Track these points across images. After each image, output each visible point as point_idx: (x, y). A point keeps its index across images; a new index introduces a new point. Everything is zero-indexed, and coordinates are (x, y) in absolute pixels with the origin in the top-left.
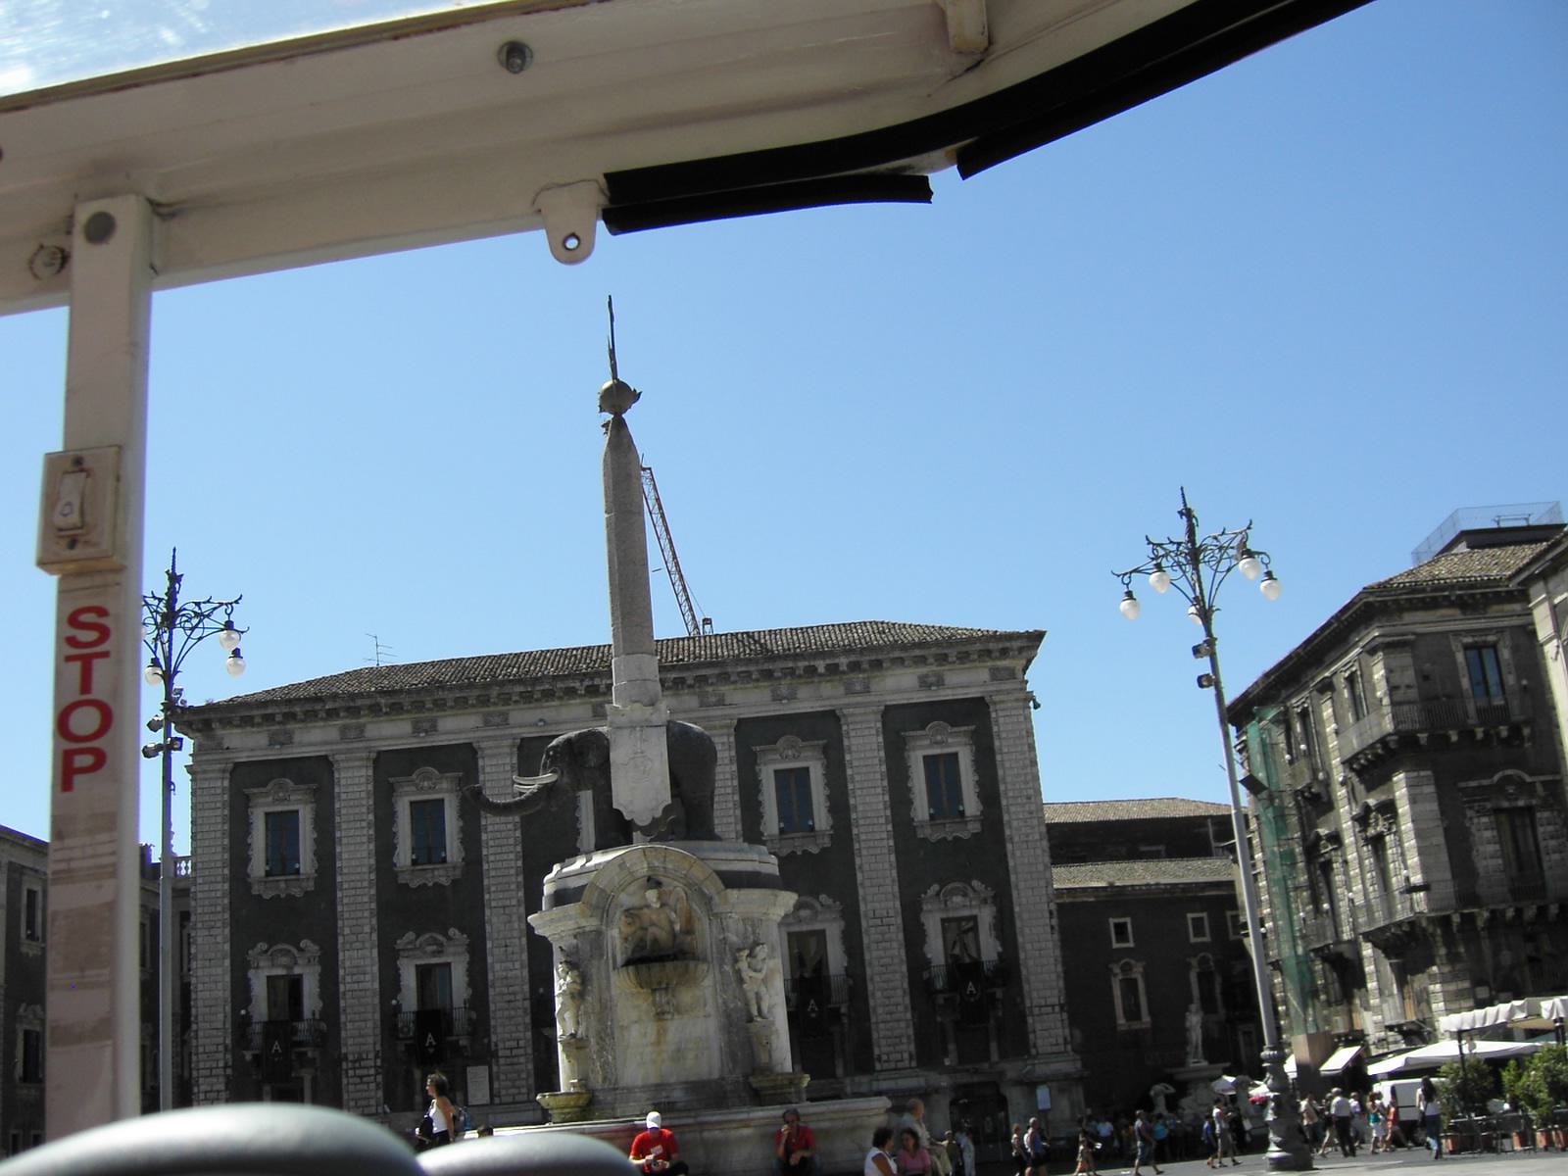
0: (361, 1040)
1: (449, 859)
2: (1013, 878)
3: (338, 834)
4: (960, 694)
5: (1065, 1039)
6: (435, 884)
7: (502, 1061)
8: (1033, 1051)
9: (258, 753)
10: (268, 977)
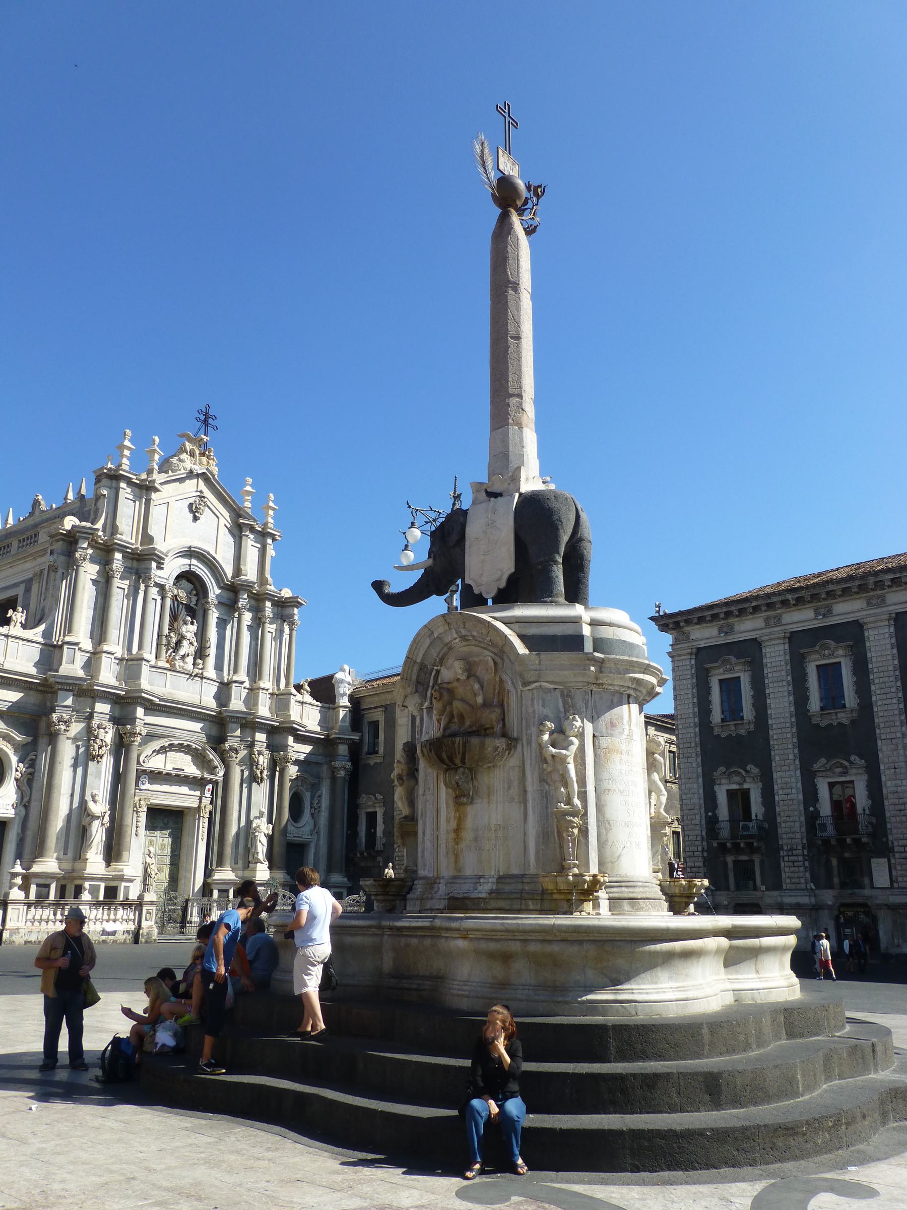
0: (791, 835)
1: (847, 705)
3: (767, 691)
6: (839, 723)
7: (897, 855)
9: (712, 640)
10: (727, 790)
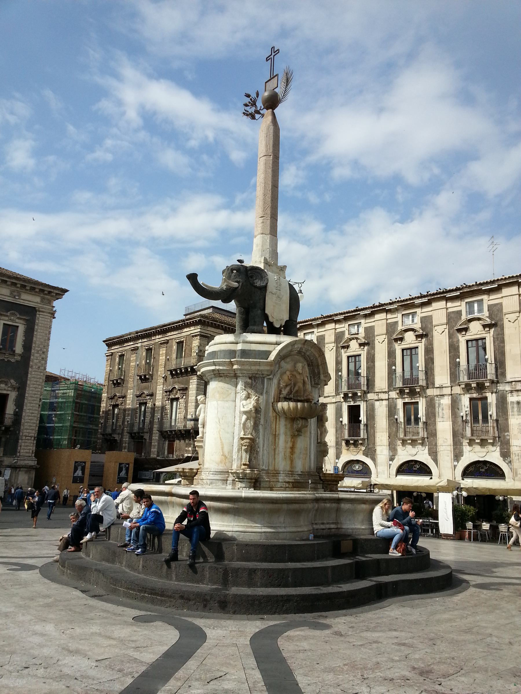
2: (28, 382)
4: (26, 303)
5: (33, 451)
8: (18, 454)
